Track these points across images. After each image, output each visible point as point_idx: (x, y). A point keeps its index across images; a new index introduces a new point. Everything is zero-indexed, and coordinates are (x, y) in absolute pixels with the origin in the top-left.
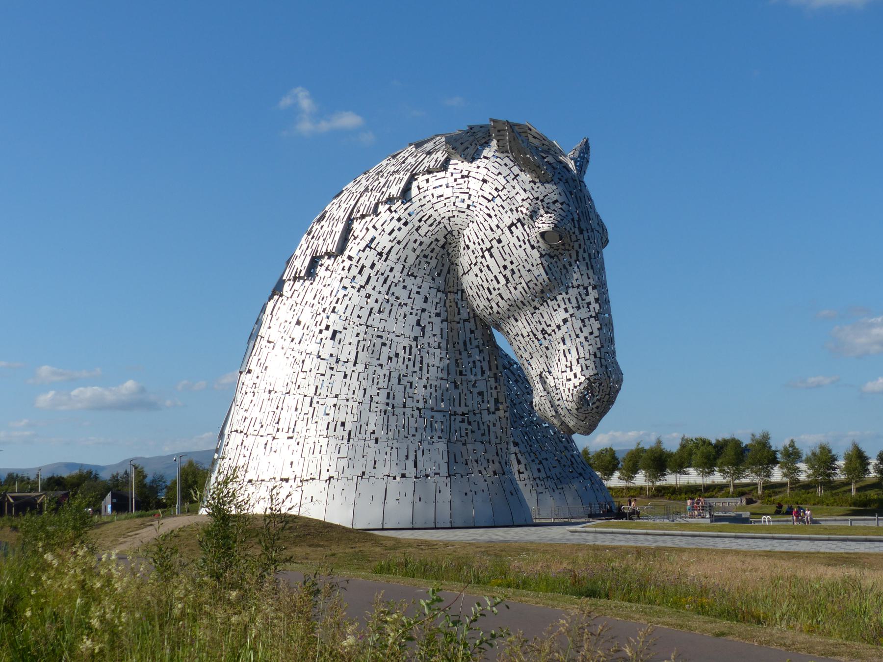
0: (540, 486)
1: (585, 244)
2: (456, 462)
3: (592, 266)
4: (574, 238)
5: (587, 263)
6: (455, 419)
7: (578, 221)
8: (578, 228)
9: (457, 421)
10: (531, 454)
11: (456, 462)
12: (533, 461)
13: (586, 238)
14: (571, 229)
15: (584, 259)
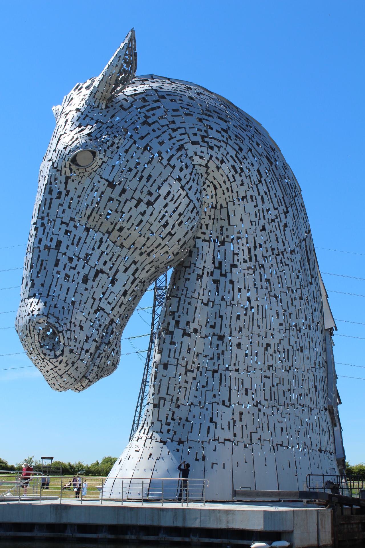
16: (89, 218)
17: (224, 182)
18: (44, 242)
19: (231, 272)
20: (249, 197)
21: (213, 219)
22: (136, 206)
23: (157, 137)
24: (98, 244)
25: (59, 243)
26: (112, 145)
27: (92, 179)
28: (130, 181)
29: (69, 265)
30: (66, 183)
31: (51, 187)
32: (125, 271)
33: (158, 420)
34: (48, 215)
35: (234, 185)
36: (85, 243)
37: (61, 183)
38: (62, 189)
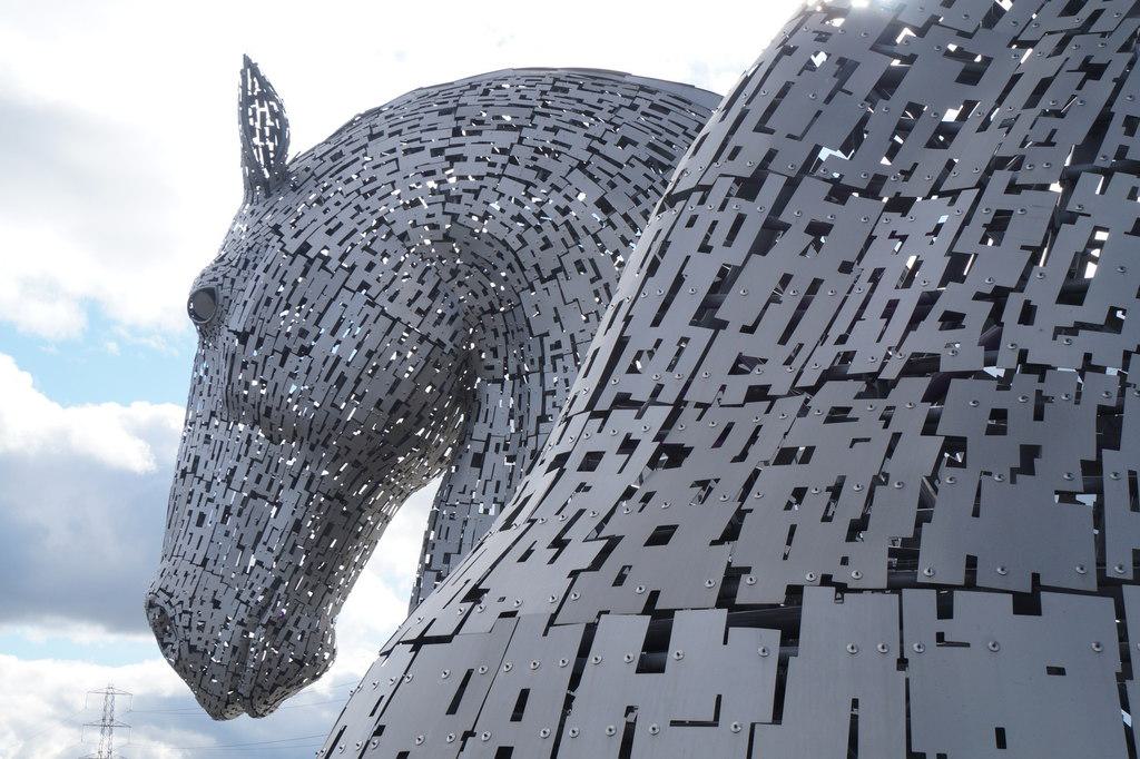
17: (500, 255)
19: (537, 433)
20: (570, 267)
21: (505, 334)
22: (282, 364)
23: (326, 224)
24: (245, 446)
26: (245, 267)
28: (269, 322)
29: (206, 495)
32: (293, 486)
35: (524, 256)
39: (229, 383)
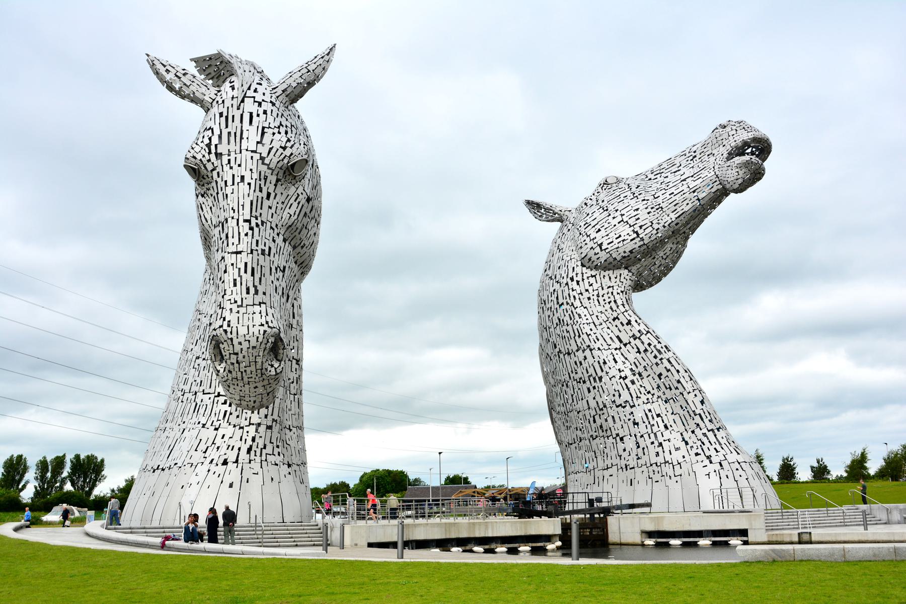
0: (656, 473)
1: (223, 171)
2: (196, 450)
3: (227, 195)
4: (210, 167)
5: (223, 193)
6: (218, 401)
7: (216, 145)
8: (216, 154)
9: (220, 403)
10: (652, 436)
11: (196, 450)
12: (652, 443)
13: (225, 161)
14: (204, 156)
15: (222, 190)
16: (288, 228)
18: (261, 246)
25: (270, 248)
27: (297, 189)
30: (276, 185)
31: (260, 184)
33: (271, 442)
34: (261, 214)
36: (283, 254)
37: (271, 183)
38: (271, 190)
39: (297, 219)
